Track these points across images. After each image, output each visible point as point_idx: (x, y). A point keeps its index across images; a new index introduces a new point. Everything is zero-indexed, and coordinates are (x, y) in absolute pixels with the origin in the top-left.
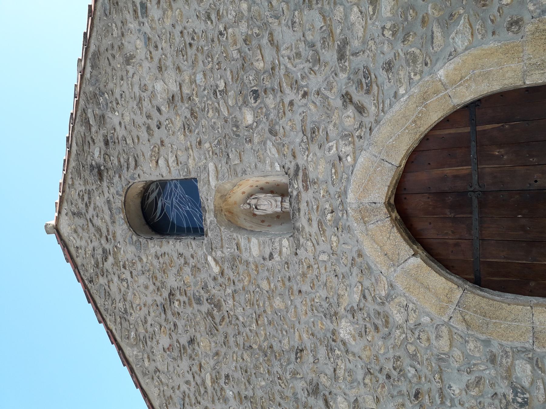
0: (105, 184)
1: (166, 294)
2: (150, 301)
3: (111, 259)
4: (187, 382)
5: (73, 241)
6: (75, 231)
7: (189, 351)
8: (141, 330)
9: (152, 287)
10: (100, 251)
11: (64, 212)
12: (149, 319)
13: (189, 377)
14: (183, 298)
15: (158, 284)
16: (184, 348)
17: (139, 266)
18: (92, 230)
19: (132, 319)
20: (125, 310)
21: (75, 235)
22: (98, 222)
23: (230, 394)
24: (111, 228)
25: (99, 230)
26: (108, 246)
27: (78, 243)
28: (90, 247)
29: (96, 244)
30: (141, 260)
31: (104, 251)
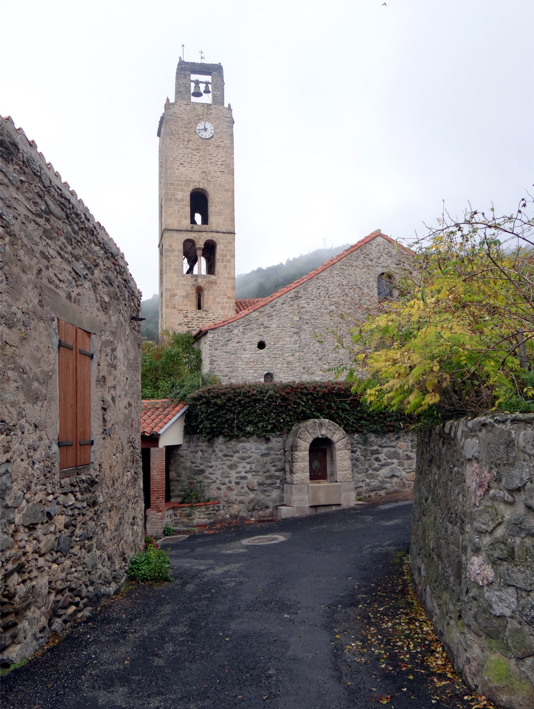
0: (395, 266)
1: (361, 286)
2: (357, 278)
3: (370, 263)
4: (332, 291)
5: (374, 243)
6: (378, 245)
7: (343, 293)
8: (346, 272)
9: (363, 280)
10: (372, 258)
11: (385, 240)
12: (351, 277)
13: (334, 292)
14: (360, 293)
15: (364, 284)
16: (344, 291)
17: (368, 276)
18: (380, 255)
19: (350, 268)
20: (352, 266)
21: (376, 244)
22: (382, 259)
23: (333, 307)
24: (380, 265)
25: (379, 258)
26: (374, 262)
27: (374, 245)
28: (373, 253)
29: (374, 255)
30: (371, 277)
31: (371, 260)
